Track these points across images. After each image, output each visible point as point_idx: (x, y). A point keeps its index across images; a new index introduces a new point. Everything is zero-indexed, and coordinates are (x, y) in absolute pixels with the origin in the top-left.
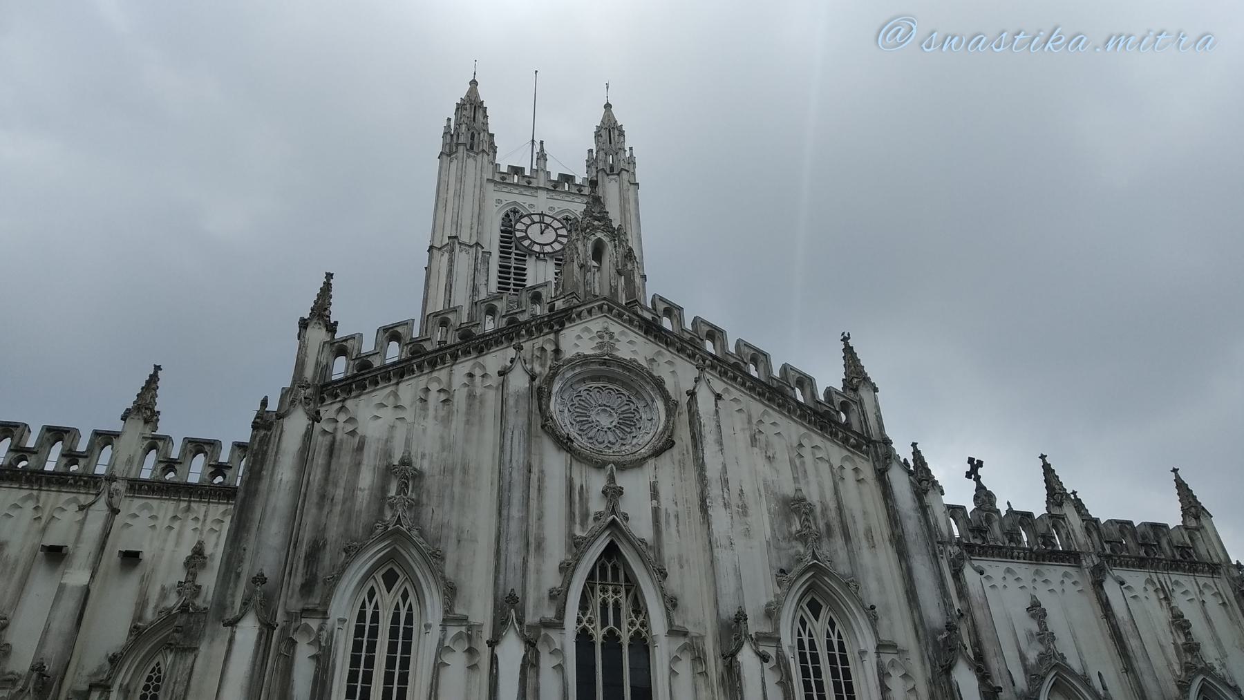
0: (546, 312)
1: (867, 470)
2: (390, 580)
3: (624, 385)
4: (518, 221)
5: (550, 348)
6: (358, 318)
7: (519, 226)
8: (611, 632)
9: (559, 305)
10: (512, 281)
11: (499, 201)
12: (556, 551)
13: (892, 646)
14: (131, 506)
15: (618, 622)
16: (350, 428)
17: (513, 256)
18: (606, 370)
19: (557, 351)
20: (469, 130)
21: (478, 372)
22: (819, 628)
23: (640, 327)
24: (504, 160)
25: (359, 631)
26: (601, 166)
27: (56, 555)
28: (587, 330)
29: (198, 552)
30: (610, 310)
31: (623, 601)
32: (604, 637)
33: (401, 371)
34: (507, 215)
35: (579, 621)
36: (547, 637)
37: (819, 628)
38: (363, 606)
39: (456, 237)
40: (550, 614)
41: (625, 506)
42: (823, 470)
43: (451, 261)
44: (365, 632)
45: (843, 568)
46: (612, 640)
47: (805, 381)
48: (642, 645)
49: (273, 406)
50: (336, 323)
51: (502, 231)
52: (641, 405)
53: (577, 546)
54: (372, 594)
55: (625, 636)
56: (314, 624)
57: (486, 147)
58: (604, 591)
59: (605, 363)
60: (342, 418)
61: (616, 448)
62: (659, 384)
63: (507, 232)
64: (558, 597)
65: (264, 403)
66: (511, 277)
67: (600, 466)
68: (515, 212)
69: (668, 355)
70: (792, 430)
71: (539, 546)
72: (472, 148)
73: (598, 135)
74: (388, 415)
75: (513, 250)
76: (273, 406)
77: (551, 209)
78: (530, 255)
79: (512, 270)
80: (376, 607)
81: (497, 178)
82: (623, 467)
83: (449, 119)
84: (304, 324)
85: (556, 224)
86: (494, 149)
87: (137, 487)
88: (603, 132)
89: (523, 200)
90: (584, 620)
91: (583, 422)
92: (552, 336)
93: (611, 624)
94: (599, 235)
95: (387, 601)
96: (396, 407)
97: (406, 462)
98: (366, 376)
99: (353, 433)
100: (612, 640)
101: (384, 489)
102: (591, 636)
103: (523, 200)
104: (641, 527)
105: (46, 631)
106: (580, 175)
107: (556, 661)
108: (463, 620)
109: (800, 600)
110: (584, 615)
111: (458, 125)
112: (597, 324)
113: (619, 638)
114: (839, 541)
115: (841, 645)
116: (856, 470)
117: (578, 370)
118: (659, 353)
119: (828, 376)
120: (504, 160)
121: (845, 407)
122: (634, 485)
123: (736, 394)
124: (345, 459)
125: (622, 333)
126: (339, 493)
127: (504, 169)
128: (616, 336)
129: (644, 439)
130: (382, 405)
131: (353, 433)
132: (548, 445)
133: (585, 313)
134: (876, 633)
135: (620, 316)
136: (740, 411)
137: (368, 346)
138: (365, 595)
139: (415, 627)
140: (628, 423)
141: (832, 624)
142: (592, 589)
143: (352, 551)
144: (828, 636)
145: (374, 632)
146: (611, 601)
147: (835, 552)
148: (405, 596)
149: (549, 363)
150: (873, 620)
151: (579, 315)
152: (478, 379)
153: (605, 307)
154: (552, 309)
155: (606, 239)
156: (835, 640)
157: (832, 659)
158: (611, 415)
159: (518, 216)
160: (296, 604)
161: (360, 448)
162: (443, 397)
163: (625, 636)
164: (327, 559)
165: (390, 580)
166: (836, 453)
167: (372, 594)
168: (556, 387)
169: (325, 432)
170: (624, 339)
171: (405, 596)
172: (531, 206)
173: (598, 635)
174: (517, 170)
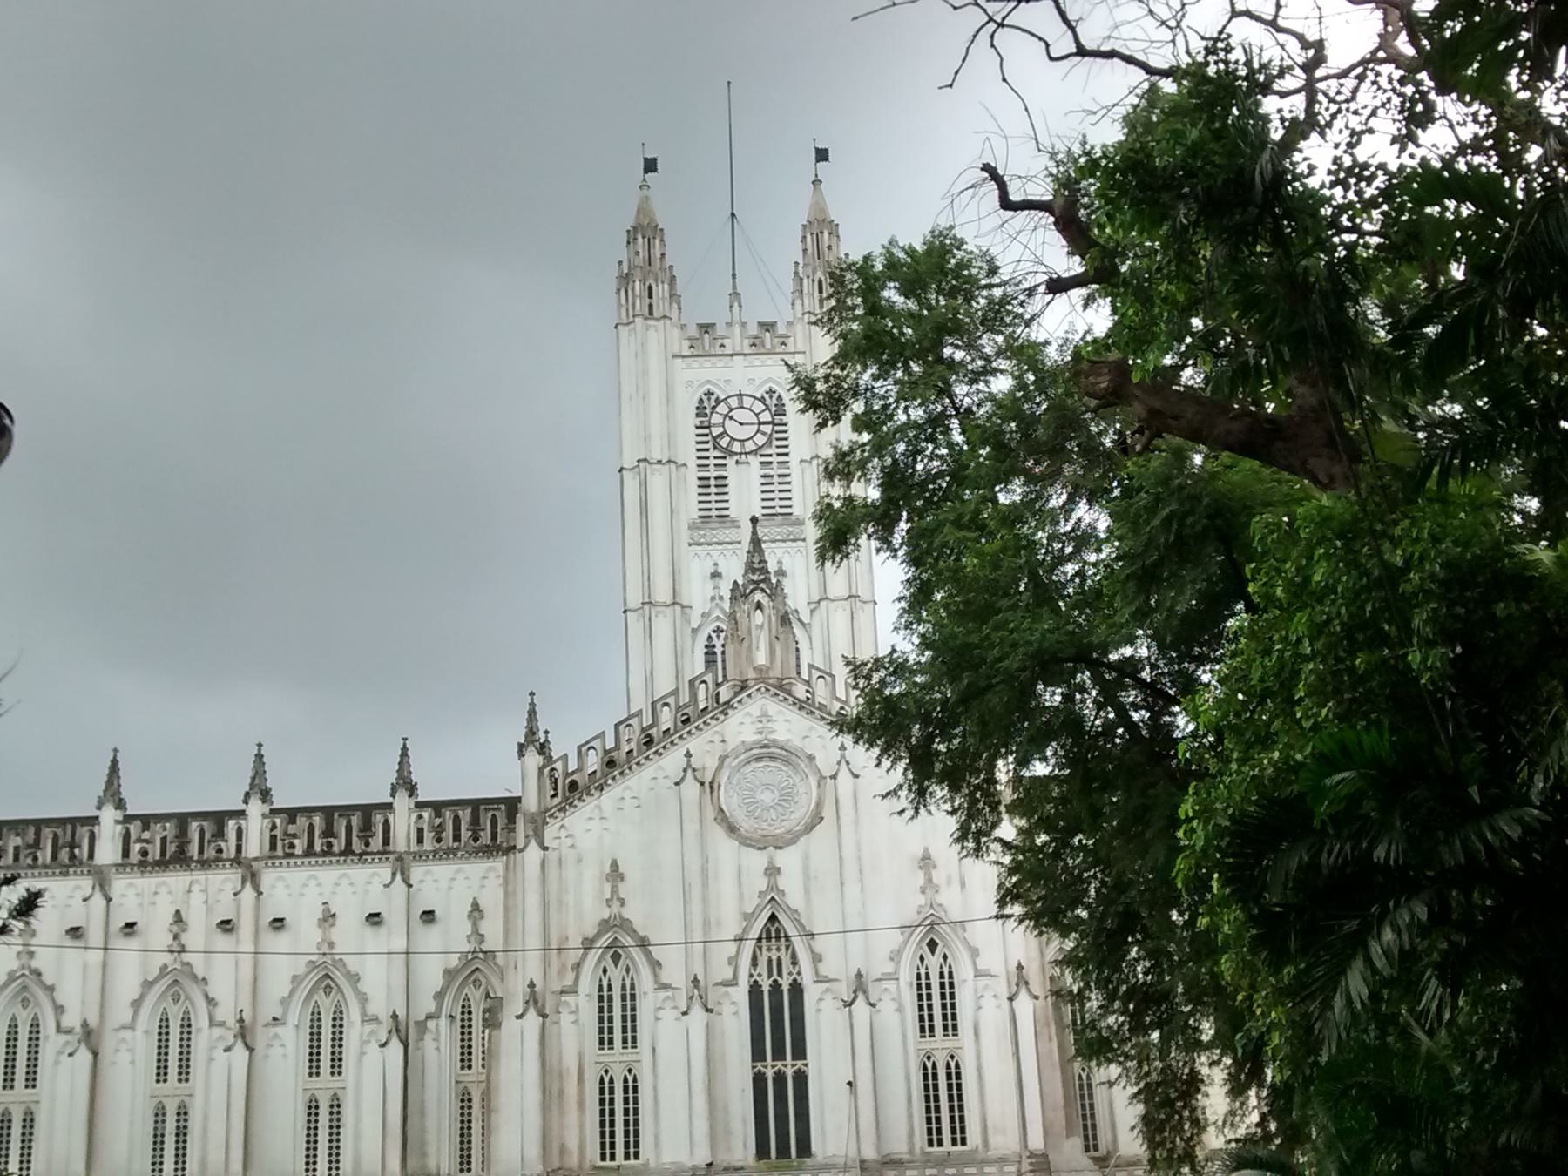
2: (616, 958)
3: (785, 761)
5: (717, 739)
8: (775, 981)
12: (732, 928)
14: (417, 872)
15: (780, 974)
16: (569, 842)
18: (768, 752)
21: (660, 774)
22: (933, 962)
25: (601, 998)
27: (374, 918)
29: (476, 906)
33: (598, 784)
36: (727, 994)
37: (933, 962)
40: (729, 975)
44: (604, 999)
46: (776, 987)
48: (797, 989)
52: (797, 779)
53: (749, 918)
54: (605, 971)
55: (785, 984)
56: (570, 999)
59: (765, 746)
60: (563, 833)
61: (777, 824)
62: (811, 758)
64: (734, 961)
71: (718, 923)
84: (521, 749)
87: (418, 856)
93: (775, 976)
95: (616, 975)
97: (615, 865)
98: (573, 790)
99: (572, 846)
100: (776, 987)
101: (602, 892)
104: (794, 899)
105: (388, 986)
107: (733, 1009)
108: (666, 986)
114: (956, 886)
115: (951, 974)
122: (788, 859)
124: (570, 872)
126: (570, 898)
129: (800, 813)
132: (718, 833)
134: (974, 964)
140: (786, 798)
141: (945, 957)
145: (610, 999)
146: (774, 958)
148: (628, 970)
152: (661, 780)
156: (946, 970)
157: (942, 985)
161: (580, 861)
163: (785, 988)
165: (616, 958)
167: (605, 971)
168: (723, 778)
171: (628, 970)
173: (766, 986)
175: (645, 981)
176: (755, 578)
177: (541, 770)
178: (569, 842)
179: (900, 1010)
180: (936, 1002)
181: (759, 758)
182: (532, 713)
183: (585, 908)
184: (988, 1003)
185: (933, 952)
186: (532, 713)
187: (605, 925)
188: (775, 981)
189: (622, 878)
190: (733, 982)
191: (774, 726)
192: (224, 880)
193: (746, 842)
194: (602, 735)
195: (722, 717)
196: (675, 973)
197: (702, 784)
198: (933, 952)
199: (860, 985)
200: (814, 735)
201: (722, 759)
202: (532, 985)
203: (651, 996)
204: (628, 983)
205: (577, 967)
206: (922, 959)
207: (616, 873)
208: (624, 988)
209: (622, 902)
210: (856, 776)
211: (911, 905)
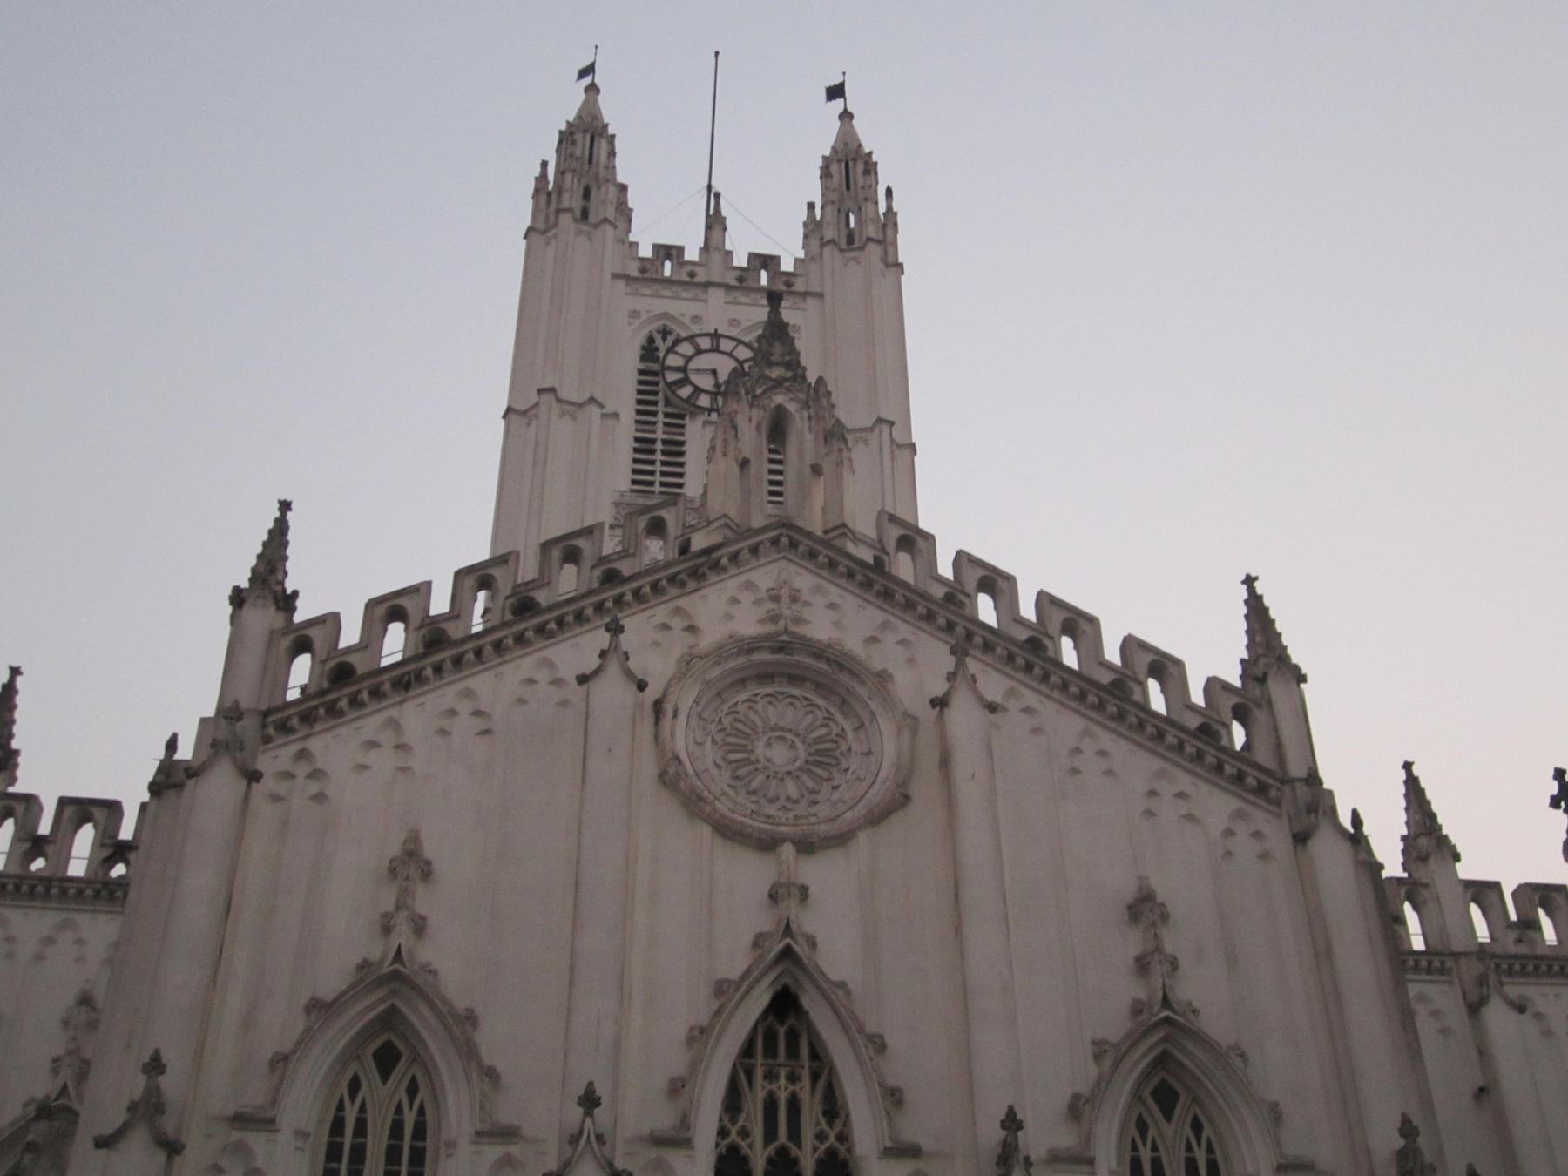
0: (673, 554)
1: (1278, 836)
2: (386, 1060)
3: (818, 687)
4: (670, 350)
6: (332, 586)
7: (673, 360)
8: (783, 1151)
9: (699, 542)
10: (658, 467)
11: (635, 314)
12: (687, 1004)
15: (795, 1134)
16: (314, 787)
17: (660, 418)
19: (691, 629)
23: (850, 575)
24: (646, 236)
25: (334, 1152)
26: (829, 234)
28: (749, 586)
30: (794, 545)
31: (805, 1095)
32: (770, 1161)
33: (405, 679)
34: (651, 340)
35: (723, 1133)
38: (340, 1107)
39: (552, 390)
40: (663, 1118)
41: (810, 922)
42: (1191, 841)
45: (1216, 1023)
47: (1165, 668)
49: (185, 752)
50: (295, 594)
51: (641, 372)
54: (354, 1086)
57: (610, 212)
58: (770, 1076)
60: (302, 770)
61: (801, 809)
62: (884, 677)
65: (172, 745)
66: (657, 457)
67: (767, 844)
68: (665, 333)
69: (904, 630)
70: (1137, 765)
72: (585, 213)
73: (825, 173)
74: (382, 761)
75: (661, 408)
76: (185, 752)
77: (734, 322)
78: (693, 415)
79: (659, 446)
80: (362, 1109)
81: (635, 273)
82: (806, 846)
83: (544, 164)
84: (238, 598)
86: (624, 213)
88: (834, 168)
89: (681, 308)
90: (734, 1132)
91: (740, 761)
92: (683, 602)
94: (779, 399)
95: (383, 1097)
96: (397, 747)
99: (320, 798)
102: (745, 1160)
103: (681, 308)
106: (790, 251)
108: (508, 1134)
109: (1140, 1084)
110: (733, 1121)
111: (560, 173)
112: (765, 575)
113: (795, 1162)
116: (1257, 835)
117: (731, 664)
118: (885, 626)
119: (1213, 654)
120: (646, 236)
121: (1241, 714)
123: (1031, 698)
125: (817, 590)
127: (645, 251)
128: (805, 596)
130: (372, 745)
131: (320, 798)
133: (745, 555)
135: (812, 555)
136: (1037, 731)
137: (350, 635)
138: (343, 1090)
139: (429, 1144)
140: (824, 759)
142: (749, 1074)
144: (1189, 1148)
145: (359, 1153)
146: (783, 1097)
147: (1203, 990)
148: (413, 1090)
149: (677, 652)
151: (734, 558)
153: (785, 541)
154: (684, 549)
155: (792, 407)
158: (793, 746)
159: (669, 341)
162: (479, 724)
165: (386, 1060)
166: (1217, 805)
167: (354, 1086)
168: (686, 698)
169: (276, 798)
170: (820, 601)
171: (413, 1090)
172: (696, 319)
174: (667, 252)
175: (457, 1113)
176: (775, 373)
177: (273, 637)
178: (314, 787)
181: (765, 677)
182: (278, 535)
185: (1168, 1117)
186: (278, 535)
187: (368, 976)
188: (783, 1151)
189: (427, 873)
190: (678, 1139)
191: (807, 613)
193: (727, 831)
194: (422, 590)
195: (692, 585)
197: (642, 686)
198: (1168, 1116)
200: (889, 639)
201: (688, 662)
202: (155, 1066)
203: (465, 1148)
204: (409, 1119)
206: (1142, 1127)
207: (411, 865)
208: (397, 1129)
209: (420, 927)
210: (992, 708)
211: (1113, 998)
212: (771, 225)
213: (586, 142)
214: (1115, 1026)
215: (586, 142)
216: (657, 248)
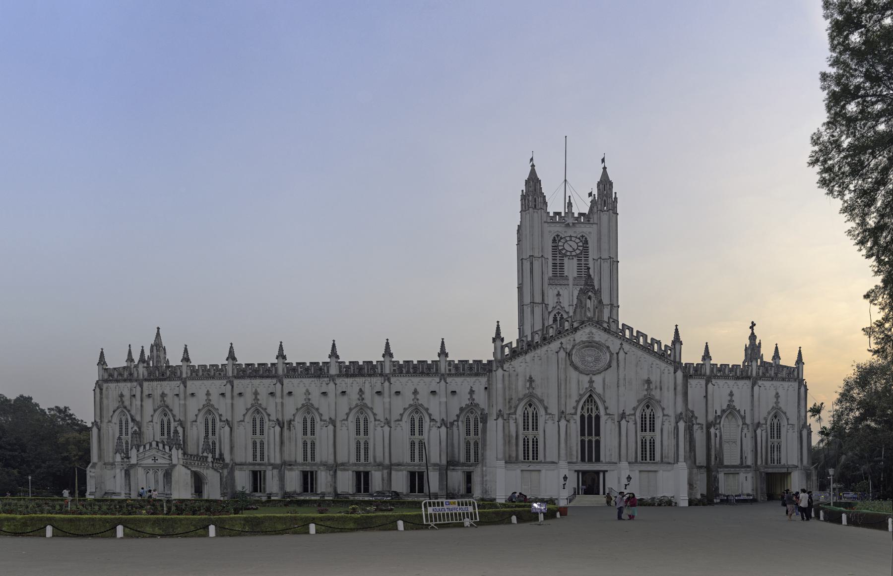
2: (530, 405)
7: (560, 244)
11: (550, 232)
12: (575, 397)
13: (667, 415)
20: (533, 194)
22: (648, 412)
24: (551, 210)
37: (648, 412)
40: (573, 411)
43: (532, 264)
46: (590, 417)
48: (598, 418)
55: (593, 416)
63: (555, 248)
64: (576, 408)
68: (558, 236)
85: (578, 241)
86: (545, 203)
95: (530, 410)
100: (590, 417)
104: (599, 388)
120: (551, 210)
127: (551, 214)
143: (520, 400)
150: (663, 409)
160: (508, 412)
164: (513, 401)
165: (530, 405)
173: (586, 415)
175: (542, 412)
179: (636, 424)
180: (648, 422)
183: (521, 388)
184: (666, 424)
192: (377, 381)
196: (554, 410)
199: (623, 416)
205: (516, 407)
212: (582, 206)
213: (533, 181)
214: (641, 396)
215: (533, 181)
216: (555, 213)
